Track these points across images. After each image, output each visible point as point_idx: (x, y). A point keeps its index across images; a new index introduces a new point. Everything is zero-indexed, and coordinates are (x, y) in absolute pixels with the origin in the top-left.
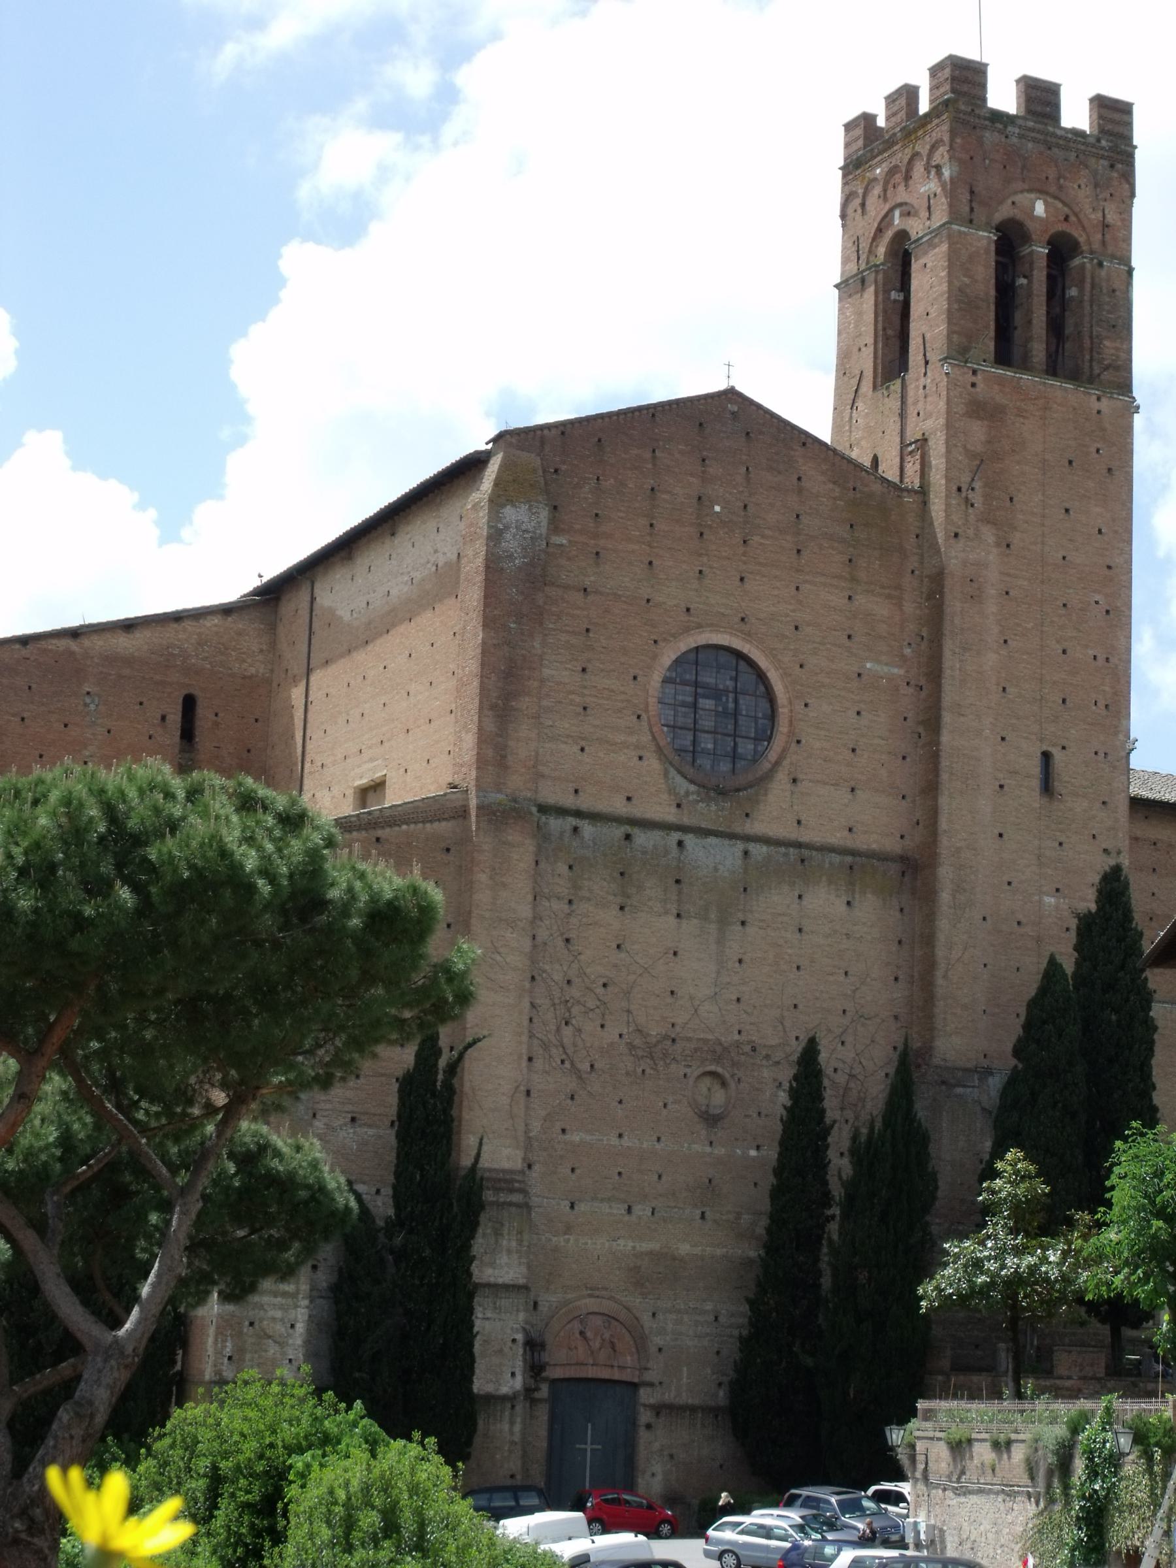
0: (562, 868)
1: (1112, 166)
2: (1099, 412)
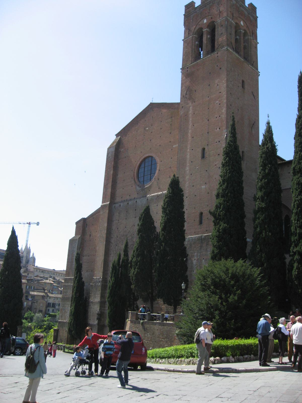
0: (118, 214)
2: (218, 56)
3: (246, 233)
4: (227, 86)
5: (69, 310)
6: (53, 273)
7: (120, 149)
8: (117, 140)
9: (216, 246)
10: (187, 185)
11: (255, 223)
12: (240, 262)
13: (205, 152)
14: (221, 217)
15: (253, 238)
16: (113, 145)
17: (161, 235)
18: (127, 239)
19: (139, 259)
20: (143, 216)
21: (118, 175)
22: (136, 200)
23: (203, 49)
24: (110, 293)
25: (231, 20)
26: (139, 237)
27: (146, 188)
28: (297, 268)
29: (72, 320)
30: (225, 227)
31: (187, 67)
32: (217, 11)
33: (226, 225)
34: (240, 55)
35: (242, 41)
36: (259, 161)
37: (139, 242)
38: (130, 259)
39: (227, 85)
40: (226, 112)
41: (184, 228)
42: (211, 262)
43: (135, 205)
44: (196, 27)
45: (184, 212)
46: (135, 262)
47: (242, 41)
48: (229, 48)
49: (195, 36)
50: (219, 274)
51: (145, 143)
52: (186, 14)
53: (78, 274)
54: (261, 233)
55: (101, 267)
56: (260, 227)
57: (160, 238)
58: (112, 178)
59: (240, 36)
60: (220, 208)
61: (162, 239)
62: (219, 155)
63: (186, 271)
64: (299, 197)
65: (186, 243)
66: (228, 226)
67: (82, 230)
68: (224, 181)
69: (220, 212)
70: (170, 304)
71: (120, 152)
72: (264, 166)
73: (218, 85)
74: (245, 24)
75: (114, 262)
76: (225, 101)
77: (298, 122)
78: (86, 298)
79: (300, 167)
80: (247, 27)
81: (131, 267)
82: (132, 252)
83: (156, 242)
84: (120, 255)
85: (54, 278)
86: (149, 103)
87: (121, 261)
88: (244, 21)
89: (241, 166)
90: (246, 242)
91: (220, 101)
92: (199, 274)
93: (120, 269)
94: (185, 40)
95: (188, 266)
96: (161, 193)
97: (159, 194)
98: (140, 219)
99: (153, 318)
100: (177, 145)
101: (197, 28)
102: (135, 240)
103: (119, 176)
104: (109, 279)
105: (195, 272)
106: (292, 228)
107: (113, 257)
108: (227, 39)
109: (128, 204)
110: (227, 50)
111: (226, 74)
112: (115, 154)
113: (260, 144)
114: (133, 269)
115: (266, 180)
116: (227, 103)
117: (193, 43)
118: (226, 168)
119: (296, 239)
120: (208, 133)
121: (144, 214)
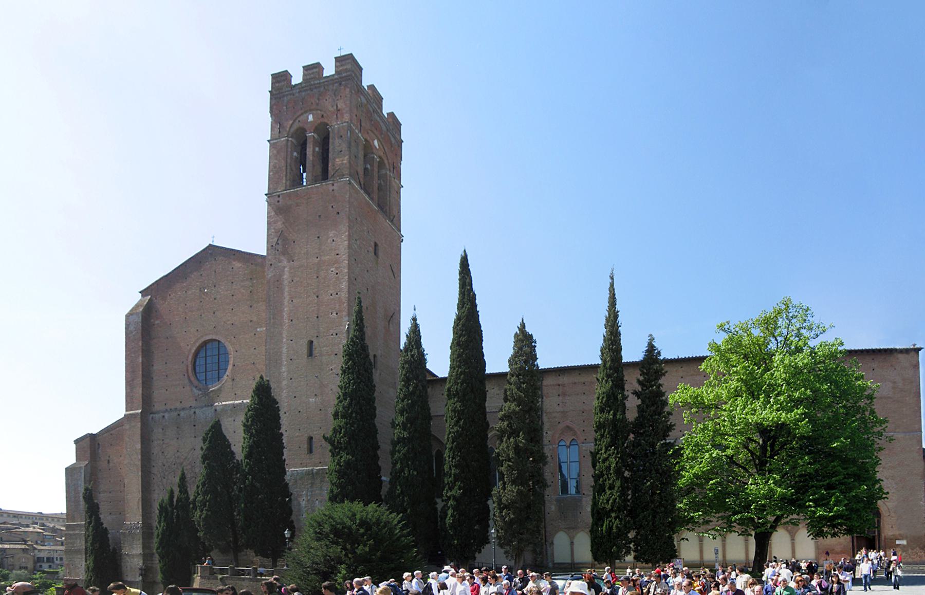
1: (340, 84)
3: (380, 470)
4: (350, 247)
5: (83, 565)
6: (39, 518)
7: (152, 321)
8: (145, 303)
9: (335, 483)
10: (284, 394)
11: (393, 457)
12: (372, 506)
13: (314, 347)
14: (343, 445)
15: (390, 476)
16: (138, 311)
17: (244, 465)
18: (183, 469)
19: (208, 498)
20: (209, 435)
21: (153, 365)
22: (193, 410)
23: (307, 170)
24: (161, 543)
25: (357, 131)
26: (205, 467)
27: (211, 391)
28: (451, 516)
29: (91, 577)
30: (349, 460)
31: (278, 194)
32: (333, 106)
33: (351, 457)
34: (372, 199)
35: (376, 174)
36: (400, 373)
37: (207, 474)
38: (192, 498)
39: (349, 243)
40: (348, 290)
41: (283, 458)
42: (329, 504)
43: (192, 417)
44: (293, 123)
45: (282, 434)
46: (201, 501)
47: (376, 174)
48: (353, 182)
49: (291, 141)
50: (341, 519)
51: (203, 315)
52: (274, 92)
53: (93, 518)
54: (402, 470)
55: (138, 508)
56: (401, 463)
57: (244, 468)
58: (141, 370)
59: (372, 166)
60: (340, 433)
61: (247, 470)
62: (336, 354)
63: (291, 514)
64: (455, 429)
65: (287, 478)
66: (354, 459)
67: (91, 453)
68: (345, 394)
69: (340, 439)
70: (265, 555)
71: (154, 325)
72: (407, 381)
73: (333, 241)
74: (381, 146)
75: (163, 501)
76: (346, 271)
77: (457, 325)
78: (114, 549)
79: (457, 388)
80: (385, 153)
81: (195, 508)
82: (195, 487)
83: (237, 474)
84: (172, 492)
85: (43, 525)
86: (207, 245)
87: (175, 500)
88: (379, 141)
89: (372, 376)
90: (381, 482)
91: (337, 268)
92: (311, 519)
93: (175, 511)
94: (272, 142)
95: (293, 508)
96: (240, 401)
97: (237, 404)
98: (204, 440)
99: (239, 573)
100: (264, 329)
101: (296, 126)
102: (198, 472)
103: (155, 368)
104: (155, 524)
105: (304, 516)
106: (445, 467)
107: (158, 494)
108: (350, 163)
109: (179, 415)
110: (350, 183)
111: (347, 224)
112: (143, 330)
113: (402, 348)
114: (198, 510)
115: (410, 401)
116: (349, 274)
117: (289, 153)
118: (349, 377)
119: (451, 481)
120: (317, 317)
121: (211, 433)
